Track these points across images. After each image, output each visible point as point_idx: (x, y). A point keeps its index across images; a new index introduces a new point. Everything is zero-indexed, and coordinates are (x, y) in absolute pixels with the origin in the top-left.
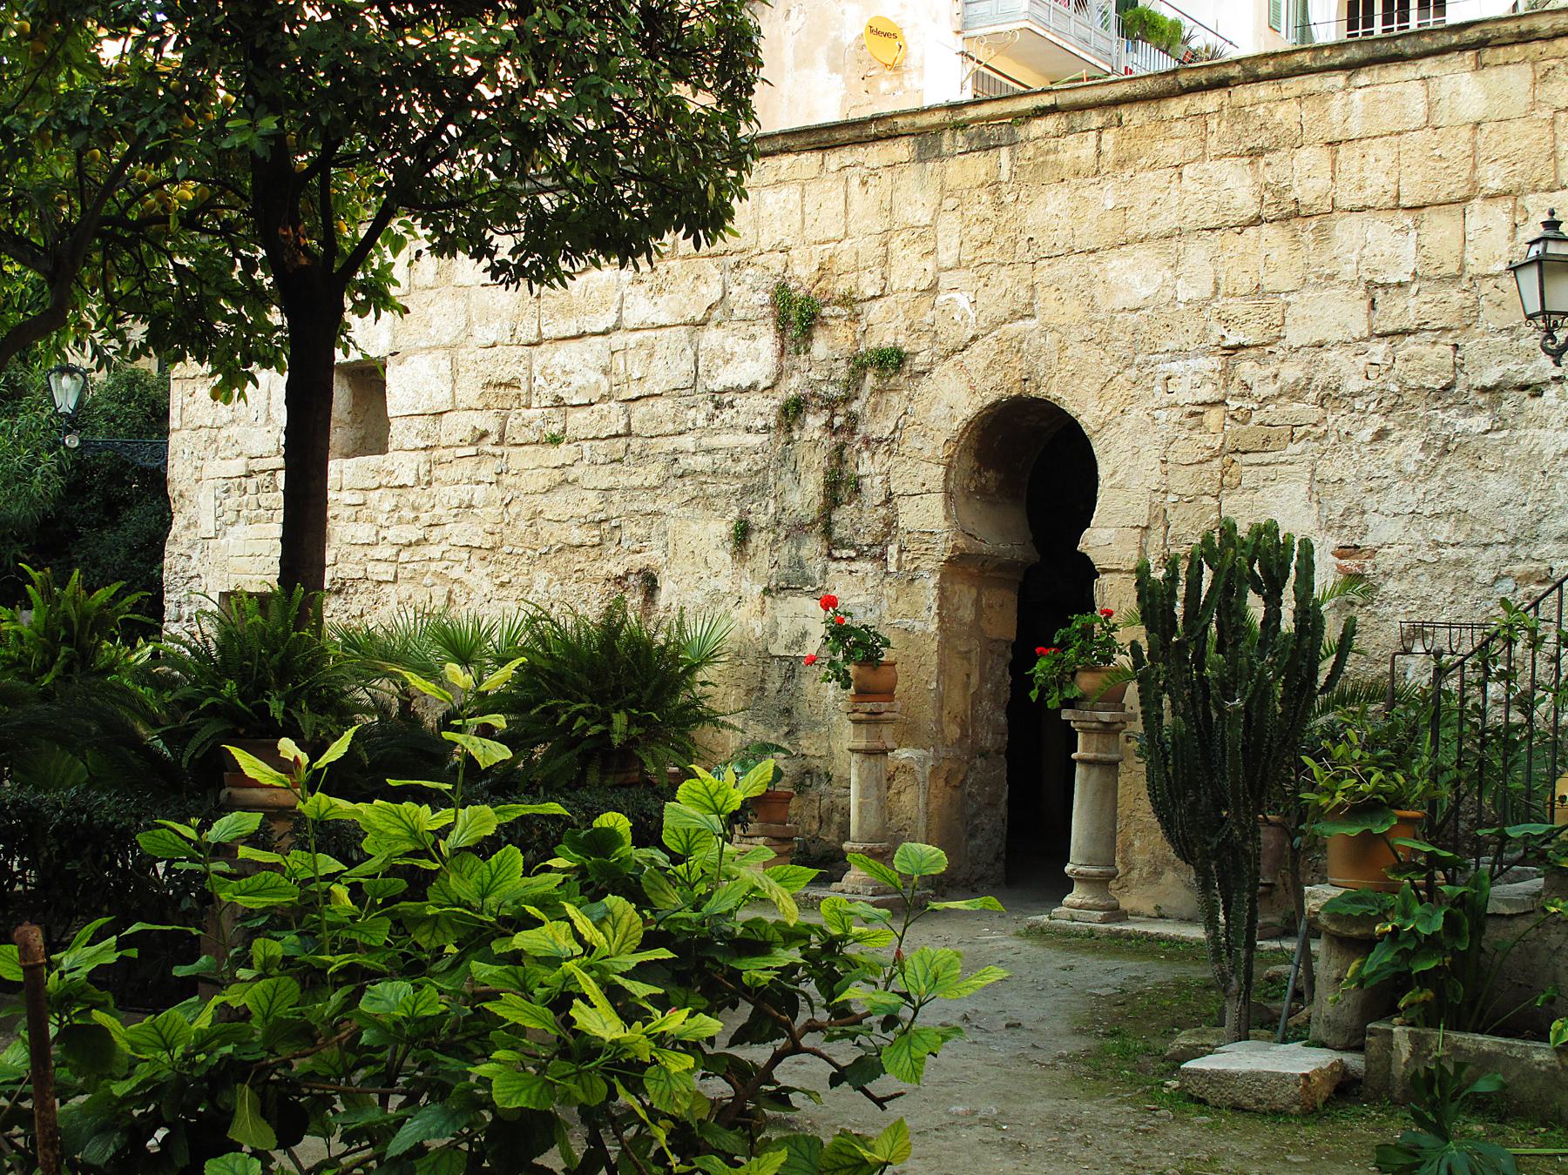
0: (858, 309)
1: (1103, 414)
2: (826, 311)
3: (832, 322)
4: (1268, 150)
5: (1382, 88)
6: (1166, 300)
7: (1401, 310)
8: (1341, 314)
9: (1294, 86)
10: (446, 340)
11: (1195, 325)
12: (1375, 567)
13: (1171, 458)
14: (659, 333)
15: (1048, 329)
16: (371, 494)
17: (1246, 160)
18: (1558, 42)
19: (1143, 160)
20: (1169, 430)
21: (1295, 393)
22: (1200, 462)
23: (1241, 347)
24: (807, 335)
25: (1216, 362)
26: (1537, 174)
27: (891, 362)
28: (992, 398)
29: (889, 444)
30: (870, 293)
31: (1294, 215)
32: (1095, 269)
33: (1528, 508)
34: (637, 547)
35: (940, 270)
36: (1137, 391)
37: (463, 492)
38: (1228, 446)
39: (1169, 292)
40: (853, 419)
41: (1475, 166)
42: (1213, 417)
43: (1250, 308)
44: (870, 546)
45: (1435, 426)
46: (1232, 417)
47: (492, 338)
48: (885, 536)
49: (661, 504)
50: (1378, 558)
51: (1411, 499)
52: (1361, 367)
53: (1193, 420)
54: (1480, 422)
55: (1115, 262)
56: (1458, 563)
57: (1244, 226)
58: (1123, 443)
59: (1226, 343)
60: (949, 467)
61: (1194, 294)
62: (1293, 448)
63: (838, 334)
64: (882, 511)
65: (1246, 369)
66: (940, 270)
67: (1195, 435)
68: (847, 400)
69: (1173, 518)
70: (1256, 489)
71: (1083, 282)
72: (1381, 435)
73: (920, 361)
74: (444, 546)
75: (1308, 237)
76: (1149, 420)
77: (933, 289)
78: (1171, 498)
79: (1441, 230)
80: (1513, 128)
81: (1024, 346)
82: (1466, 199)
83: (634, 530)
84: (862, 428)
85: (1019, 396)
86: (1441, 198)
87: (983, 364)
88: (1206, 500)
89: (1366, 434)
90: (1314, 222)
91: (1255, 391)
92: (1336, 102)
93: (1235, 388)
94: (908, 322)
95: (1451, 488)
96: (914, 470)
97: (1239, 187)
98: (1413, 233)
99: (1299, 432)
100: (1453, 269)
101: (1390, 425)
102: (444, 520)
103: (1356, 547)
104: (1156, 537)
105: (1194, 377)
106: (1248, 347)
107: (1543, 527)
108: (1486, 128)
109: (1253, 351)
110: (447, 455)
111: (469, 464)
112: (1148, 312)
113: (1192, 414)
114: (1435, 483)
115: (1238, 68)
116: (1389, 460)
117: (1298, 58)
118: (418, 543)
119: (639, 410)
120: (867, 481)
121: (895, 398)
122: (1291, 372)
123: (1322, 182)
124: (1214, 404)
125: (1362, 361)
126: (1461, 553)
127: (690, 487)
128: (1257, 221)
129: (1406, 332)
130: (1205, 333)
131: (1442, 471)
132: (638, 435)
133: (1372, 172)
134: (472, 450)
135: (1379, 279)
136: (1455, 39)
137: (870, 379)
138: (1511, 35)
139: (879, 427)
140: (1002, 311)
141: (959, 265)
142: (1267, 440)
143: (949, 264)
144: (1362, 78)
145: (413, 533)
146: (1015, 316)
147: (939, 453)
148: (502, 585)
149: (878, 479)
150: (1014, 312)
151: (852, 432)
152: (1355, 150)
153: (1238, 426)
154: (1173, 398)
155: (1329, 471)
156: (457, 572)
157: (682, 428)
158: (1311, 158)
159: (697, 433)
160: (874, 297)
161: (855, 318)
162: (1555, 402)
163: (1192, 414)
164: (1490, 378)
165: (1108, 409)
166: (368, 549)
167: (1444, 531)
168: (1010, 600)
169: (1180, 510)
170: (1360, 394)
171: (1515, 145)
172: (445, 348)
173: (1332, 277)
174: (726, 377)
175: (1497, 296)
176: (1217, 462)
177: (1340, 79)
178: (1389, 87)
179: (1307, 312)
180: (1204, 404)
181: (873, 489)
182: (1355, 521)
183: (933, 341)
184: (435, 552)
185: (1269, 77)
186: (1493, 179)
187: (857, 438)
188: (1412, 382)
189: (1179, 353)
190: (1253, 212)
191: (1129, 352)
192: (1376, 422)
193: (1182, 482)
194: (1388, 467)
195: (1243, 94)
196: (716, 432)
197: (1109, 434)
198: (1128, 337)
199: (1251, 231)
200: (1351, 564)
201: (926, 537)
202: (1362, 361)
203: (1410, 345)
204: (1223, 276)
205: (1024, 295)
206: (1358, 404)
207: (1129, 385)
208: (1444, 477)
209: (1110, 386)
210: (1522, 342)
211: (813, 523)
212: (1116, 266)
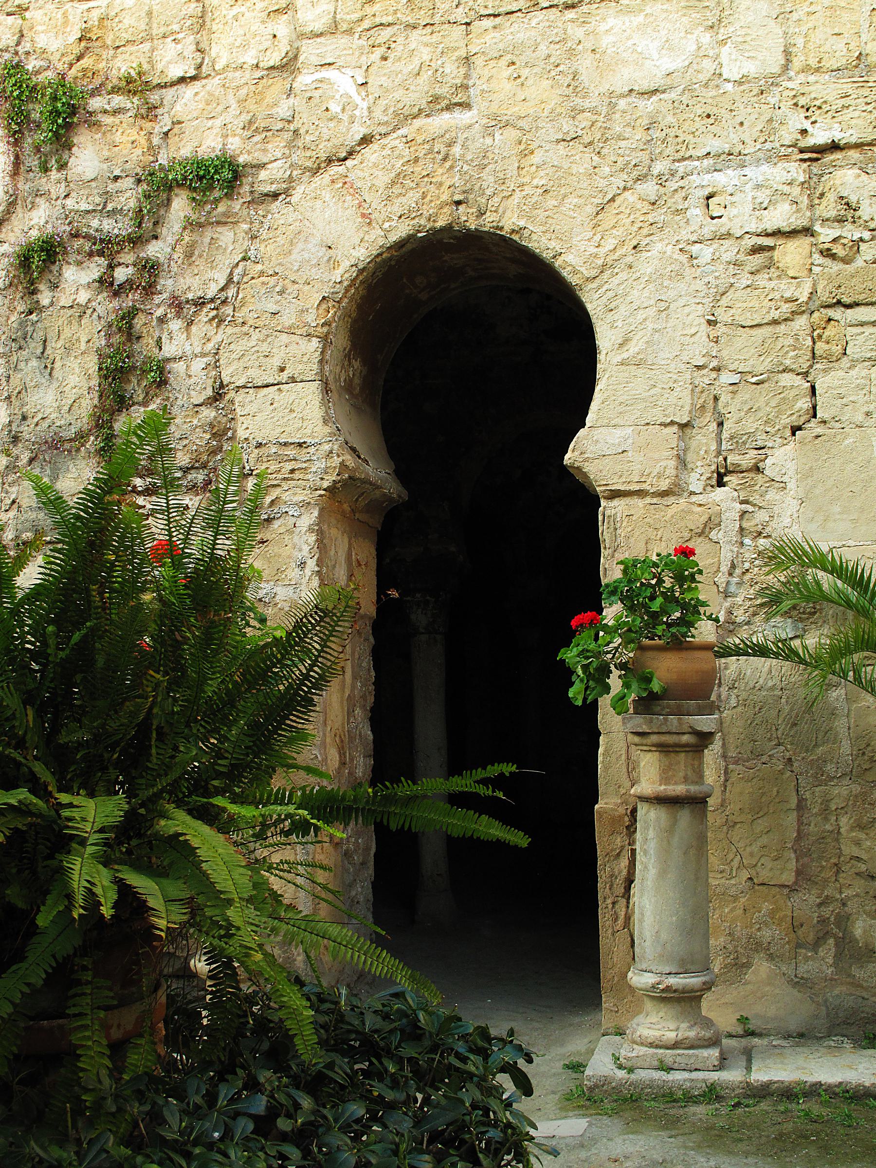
0: (154, 97)
1: (602, 251)
2: (96, 103)
3: (108, 120)
6: (703, 77)
11: (754, 117)
13: (723, 316)
15: (497, 123)
20: (721, 274)
22: (775, 322)
23: (835, 147)
24: (62, 140)
25: (797, 171)
27: (217, 180)
28: (401, 231)
29: (217, 306)
30: (176, 72)
32: (578, 32)
35: (301, 36)
36: (658, 216)
38: (824, 296)
39: (709, 66)
40: (151, 269)
42: (792, 254)
43: (848, 88)
44: (186, 470)
48: (214, 452)
53: (758, 260)
55: (611, 22)
58: (640, 295)
59: (810, 141)
60: (325, 339)
61: (751, 68)
63: (118, 137)
64: (208, 413)
66: (301, 36)
67: (762, 280)
68: (136, 241)
71: (557, 52)
73: (268, 178)
76: (684, 258)
77: (288, 66)
78: (727, 378)
81: (457, 150)
84: (166, 284)
85: (448, 228)
87: (383, 179)
88: (787, 379)
91: (865, 212)
93: (829, 208)
94: (246, 117)
96: (265, 347)
104: (703, 440)
105: (759, 194)
106: (848, 147)
109: (854, 154)
112: (673, 95)
113: (757, 250)
120: (179, 367)
121: (226, 236)
124: (793, 233)
130: (771, 126)
137: (180, 206)
139: (203, 280)
140: (417, 96)
141: (333, 29)
143: (318, 27)
146: (438, 104)
147: (310, 318)
149: (198, 365)
150: (436, 99)
151: (150, 290)
153: (835, 267)
154: (723, 225)
160: (182, 80)
161: (150, 112)
163: (757, 250)
165: (610, 243)
169: (746, 393)
176: (802, 322)
180: (777, 233)
181: (191, 380)
183: (290, 145)
187: (157, 299)
189: (731, 157)
191: (644, 157)
193: (743, 352)
197: (615, 281)
198: (640, 134)
204: (800, 42)
205: (452, 71)
207: (647, 207)
209: (612, 209)
211: (81, 437)
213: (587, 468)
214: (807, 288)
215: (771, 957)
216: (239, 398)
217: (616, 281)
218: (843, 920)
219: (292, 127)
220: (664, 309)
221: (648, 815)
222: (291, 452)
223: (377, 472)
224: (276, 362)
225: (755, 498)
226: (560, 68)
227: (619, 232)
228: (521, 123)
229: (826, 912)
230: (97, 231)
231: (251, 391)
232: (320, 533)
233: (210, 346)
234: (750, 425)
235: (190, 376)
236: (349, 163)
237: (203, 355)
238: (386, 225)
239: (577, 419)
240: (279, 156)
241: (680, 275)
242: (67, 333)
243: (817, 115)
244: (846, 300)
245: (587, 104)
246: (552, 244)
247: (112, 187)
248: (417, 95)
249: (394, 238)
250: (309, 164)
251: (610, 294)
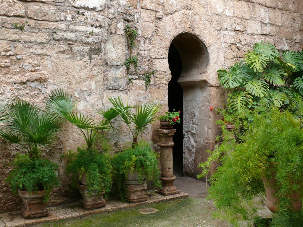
22: (232, 59)
23: (238, 30)
28: (181, 31)
34: (33, 69)
53: (229, 47)
59: (236, 29)
85: (188, 32)
87: (179, 20)
91: (242, 42)
96: (158, 50)
135: (263, 21)
157: (58, 19)
159: (66, 23)
165: (212, 41)
173: (255, 18)
176: (234, 59)
180: (233, 44)
196: (75, 24)
201: (164, 73)
216: (154, 60)
217: (212, 48)
219: (163, 5)
226: (205, 6)
227: (213, 39)
228: (200, 15)
230: (125, 18)
231: (156, 59)
233: (149, 48)
235: (144, 54)
236: (173, 15)
237: (147, 50)
238: (179, 30)
240: (161, 10)
244: (240, 57)
246: (204, 39)
249: (180, 32)
250: (166, 13)
251: (212, 50)
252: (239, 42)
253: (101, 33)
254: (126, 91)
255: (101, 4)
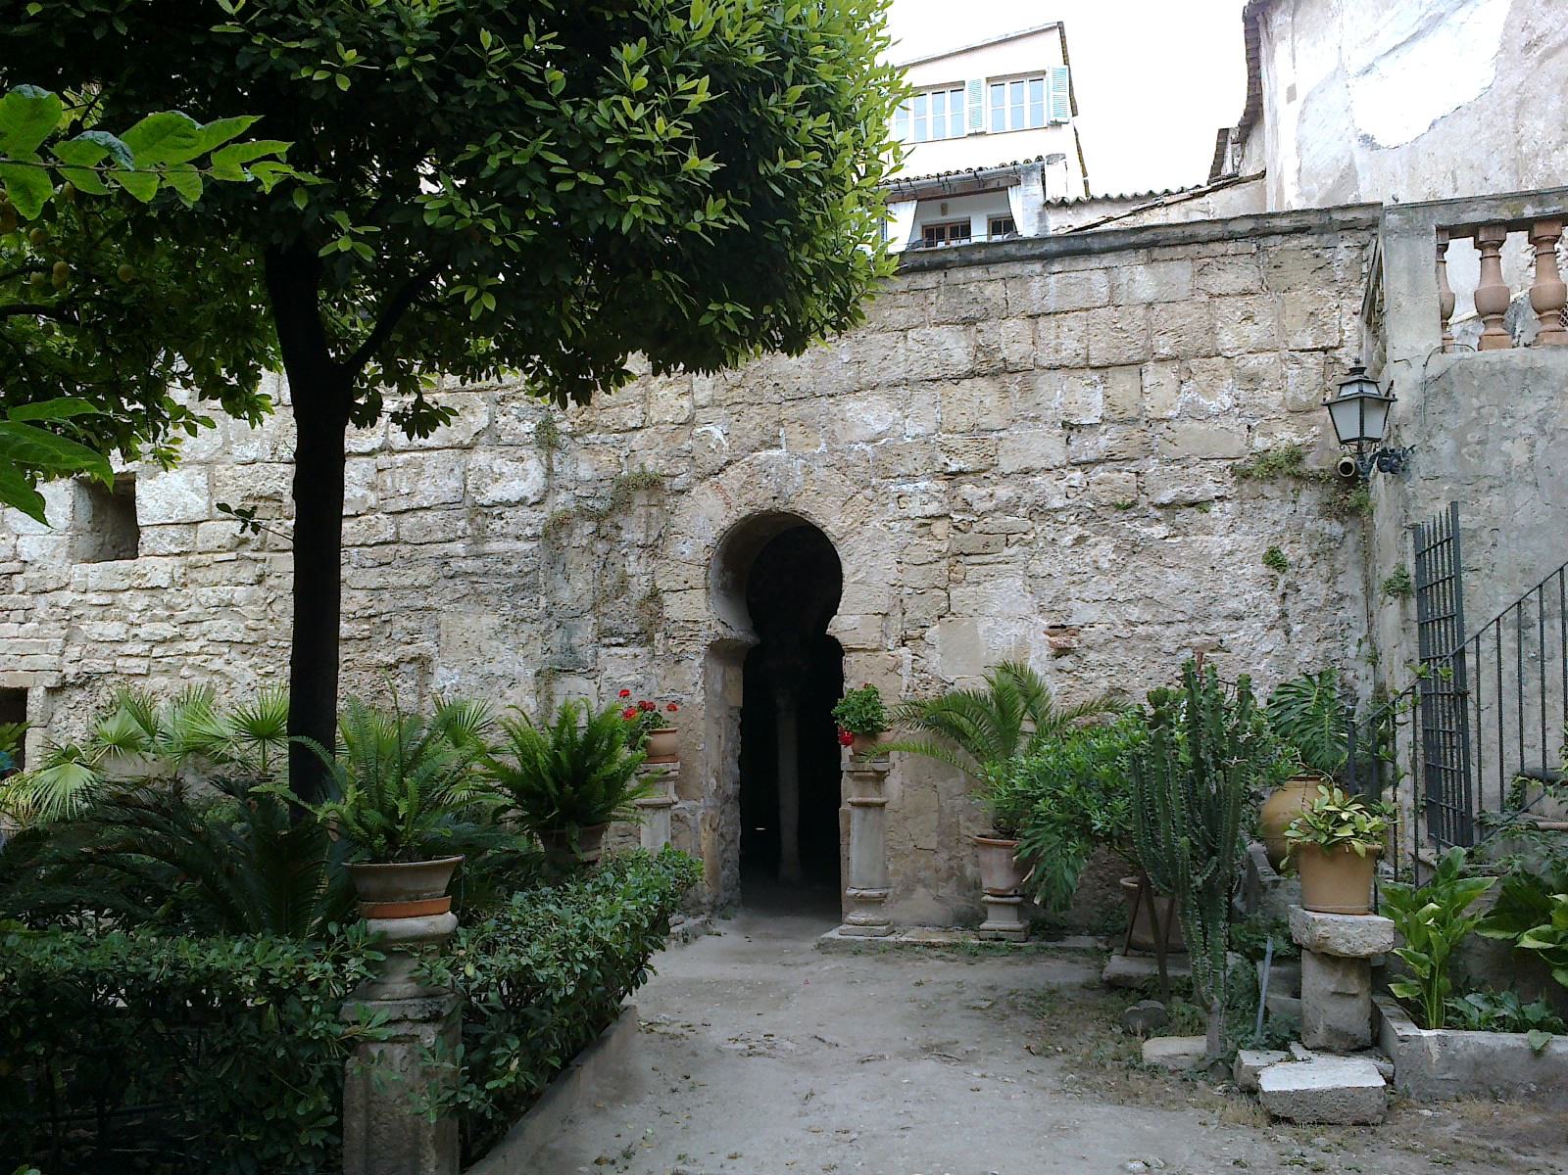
4: (979, 320)
5: (1073, 274)
7: (1091, 446)
8: (1043, 446)
9: (1001, 270)
10: (202, 456)
12: (1080, 642)
14: (426, 454)
16: (121, 595)
17: (961, 327)
18: (1211, 245)
19: (873, 325)
20: (905, 538)
21: (1009, 508)
23: (961, 472)
26: (1198, 344)
28: (746, 511)
30: (632, 424)
31: (1007, 369)
32: (834, 410)
33: (1202, 594)
34: (408, 638)
36: (873, 507)
37: (224, 592)
41: (1148, 338)
42: (940, 528)
43: (968, 442)
45: (1123, 534)
46: (955, 527)
47: (252, 454)
49: (432, 601)
50: (1082, 635)
51: (1106, 589)
52: (1063, 489)
53: (923, 530)
54: (1159, 531)
56: (1149, 638)
57: (957, 379)
59: (949, 470)
61: (920, 430)
62: (1007, 551)
65: (967, 489)
67: (925, 541)
69: (909, 603)
70: (979, 583)
72: (1080, 540)
74: (202, 642)
75: (1014, 388)
77: (690, 422)
79: (1123, 385)
80: (1180, 308)
82: (1143, 362)
83: (405, 623)
86: (1123, 361)
87: (737, 485)
88: (937, 592)
89: (1068, 540)
90: (1019, 377)
91: (976, 507)
92: (1036, 284)
95: (1139, 580)
97: (957, 348)
98: (1100, 387)
99: (1013, 539)
100: (1133, 414)
101: (1087, 533)
102: (201, 618)
103: (1063, 627)
105: (923, 496)
106: (965, 473)
107: (1212, 609)
108: (1158, 308)
109: (971, 477)
110: (206, 559)
111: (228, 568)
114: (1126, 576)
115: (956, 254)
116: (1087, 560)
117: (1007, 248)
118: (172, 640)
119: (409, 520)
122: (1004, 492)
123: (1025, 347)
125: (1062, 485)
126: (1150, 630)
127: (462, 587)
128: (972, 374)
129: (1098, 462)
131: (1131, 567)
132: (406, 543)
133: (1066, 340)
134: (233, 555)
135: (1074, 421)
136: (1133, 239)
138: (1176, 238)
141: (715, 403)
142: (987, 545)
143: (704, 403)
144: (1056, 268)
145: (167, 630)
148: (268, 674)
149: (643, 579)
152: (1052, 322)
153: (960, 535)
155: (1038, 568)
156: (217, 664)
157: (452, 536)
158: (1015, 326)
159: (468, 541)
162: (1219, 515)
164: (1165, 497)
166: (113, 646)
167: (1135, 613)
168: (735, 675)
170: (1062, 509)
171: (1180, 322)
172: (200, 463)
173: (1036, 418)
174: (494, 493)
175: (1169, 435)
176: (944, 562)
177: (1037, 267)
178: (1079, 274)
179: (1017, 446)
180: (932, 517)
182: (1062, 606)
184: (194, 647)
185: (980, 263)
186: (1164, 346)
188: (1104, 501)
189: (910, 477)
190: (965, 367)
192: (1077, 530)
193: (915, 577)
194: (1086, 565)
195: (958, 275)
199: (967, 383)
200: (1060, 640)
202: (1062, 485)
203: (1099, 472)
206: (1061, 517)
208: (1133, 572)
210: (1191, 470)
212: (853, 406)
213: (837, 636)
214: (946, 546)
215: (925, 886)
216: (665, 596)
218: (961, 868)
220: (875, 554)
221: (857, 813)
222: (690, 625)
223: (738, 632)
224: (682, 579)
225: (920, 653)
229: (953, 863)
232: (705, 668)
234: (918, 614)
239: (832, 609)
241: (882, 538)
242: (576, 560)
243: (953, 456)
245: (839, 447)
247: (599, 485)
248: (756, 436)
249: (742, 515)
252: (959, 504)
253: (536, 551)
254: (593, 674)
255: (535, 488)
